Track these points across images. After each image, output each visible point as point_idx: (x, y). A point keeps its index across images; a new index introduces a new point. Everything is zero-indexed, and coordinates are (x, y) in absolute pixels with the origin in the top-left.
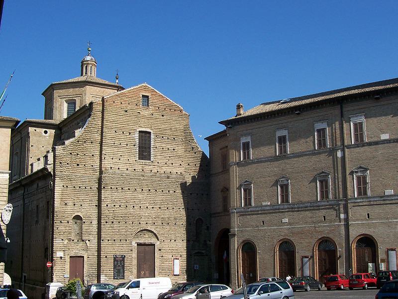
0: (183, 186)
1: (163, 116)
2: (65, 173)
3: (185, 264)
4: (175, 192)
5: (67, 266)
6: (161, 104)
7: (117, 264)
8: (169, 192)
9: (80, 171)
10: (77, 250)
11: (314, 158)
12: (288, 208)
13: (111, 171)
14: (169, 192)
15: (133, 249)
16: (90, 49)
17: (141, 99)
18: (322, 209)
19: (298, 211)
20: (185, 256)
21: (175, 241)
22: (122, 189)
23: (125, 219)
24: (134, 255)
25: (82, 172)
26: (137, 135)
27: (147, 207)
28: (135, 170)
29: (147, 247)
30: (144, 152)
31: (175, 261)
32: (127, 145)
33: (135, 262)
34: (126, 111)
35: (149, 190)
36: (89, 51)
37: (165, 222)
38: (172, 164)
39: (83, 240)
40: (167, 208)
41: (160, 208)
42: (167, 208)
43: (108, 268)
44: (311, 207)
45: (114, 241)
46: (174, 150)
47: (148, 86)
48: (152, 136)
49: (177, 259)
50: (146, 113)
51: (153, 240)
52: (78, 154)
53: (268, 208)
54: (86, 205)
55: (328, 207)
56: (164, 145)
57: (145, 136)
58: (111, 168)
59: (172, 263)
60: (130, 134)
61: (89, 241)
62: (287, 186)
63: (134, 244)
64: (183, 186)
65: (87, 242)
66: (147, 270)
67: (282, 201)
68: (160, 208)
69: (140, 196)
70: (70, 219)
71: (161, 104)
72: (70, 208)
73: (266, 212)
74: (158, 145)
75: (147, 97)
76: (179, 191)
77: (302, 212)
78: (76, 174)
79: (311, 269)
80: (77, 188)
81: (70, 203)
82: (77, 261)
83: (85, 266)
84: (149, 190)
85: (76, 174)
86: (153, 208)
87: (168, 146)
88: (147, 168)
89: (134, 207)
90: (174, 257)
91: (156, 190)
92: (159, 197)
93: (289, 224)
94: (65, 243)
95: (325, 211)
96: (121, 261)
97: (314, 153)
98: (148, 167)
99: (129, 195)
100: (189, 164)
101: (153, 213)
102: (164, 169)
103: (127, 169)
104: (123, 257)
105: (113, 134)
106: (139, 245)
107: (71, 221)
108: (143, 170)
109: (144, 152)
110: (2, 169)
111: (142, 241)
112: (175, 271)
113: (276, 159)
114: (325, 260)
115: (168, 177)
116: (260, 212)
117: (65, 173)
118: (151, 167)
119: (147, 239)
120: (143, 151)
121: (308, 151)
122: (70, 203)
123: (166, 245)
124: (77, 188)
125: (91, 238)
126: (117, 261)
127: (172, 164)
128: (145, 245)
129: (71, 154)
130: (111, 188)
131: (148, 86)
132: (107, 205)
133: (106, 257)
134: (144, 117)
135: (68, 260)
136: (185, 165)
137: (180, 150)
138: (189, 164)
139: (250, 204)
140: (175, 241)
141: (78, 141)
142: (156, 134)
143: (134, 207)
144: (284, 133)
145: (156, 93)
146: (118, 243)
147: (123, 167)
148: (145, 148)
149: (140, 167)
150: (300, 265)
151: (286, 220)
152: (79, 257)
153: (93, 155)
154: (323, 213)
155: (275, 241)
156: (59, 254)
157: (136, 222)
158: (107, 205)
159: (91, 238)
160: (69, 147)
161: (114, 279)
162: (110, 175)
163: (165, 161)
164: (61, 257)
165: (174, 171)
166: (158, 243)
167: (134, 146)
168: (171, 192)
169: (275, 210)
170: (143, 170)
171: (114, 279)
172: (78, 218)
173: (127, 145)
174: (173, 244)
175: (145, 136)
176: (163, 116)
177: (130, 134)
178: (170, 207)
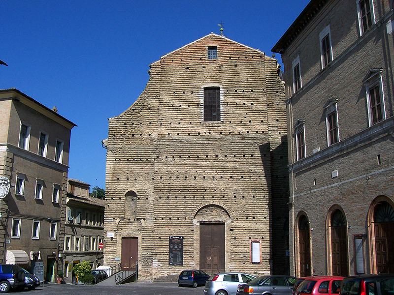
0: (265, 149)
1: (236, 66)
2: (119, 146)
3: (268, 248)
4: (252, 156)
5: (119, 248)
6: (232, 53)
7: (174, 246)
8: (244, 156)
9: (137, 141)
10: (129, 230)
11: (361, 53)
12: (337, 152)
13: (167, 138)
14: (244, 156)
15: (195, 229)
16: (222, 29)
17: (206, 52)
18: (375, 142)
19: (348, 154)
20: (267, 238)
21: (254, 218)
22: (180, 157)
23: (183, 193)
24: (196, 236)
25: (139, 142)
26: (201, 94)
27: (214, 177)
28: (199, 133)
29: (215, 228)
30: (212, 111)
31: (254, 244)
32: (189, 106)
33: (197, 245)
34: (188, 68)
35: (217, 156)
36: (222, 31)
37: (239, 195)
38: (250, 121)
39: (138, 219)
40: (242, 177)
41: (231, 177)
42: (242, 177)
43: (162, 251)
44: (361, 142)
45: (170, 219)
46: (252, 104)
47: (216, 35)
48: (222, 92)
49: (256, 242)
50: (213, 66)
51: (222, 218)
52: (133, 124)
53: (318, 157)
54: (141, 179)
55: (382, 136)
56: (244, 101)
57: (212, 94)
58: (169, 134)
59: (250, 247)
60: (192, 93)
61: (144, 219)
62: (334, 114)
63: (196, 223)
64: (265, 149)
65: (142, 220)
66: (215, 256)
67: (332, 142)
68: (231, 177)
69: (204, 164)
70: (123, 196)
71: (232, 53)
72: (122, 183)
73: (317, 163)
74: (229, 101)
75: (215, 48)
76: (258, 155)
77: (352, 155)
78: (129, 146)
79: (365, 258)
80: (131, 160)
81: (123, 178)
82: (130, 243)
83: (140, 249)
84: (217, 156)
85: (129, 146)
86: (221, 177)
87: (244, 101)
88: (216, 130)
89: (195, 177)
90: (253, 240)
91: (226, 156)
92: (231, 164)
93: (339, 178)
94: (117, 221)
95: (379, 144)
96: (178, 243)
97: (360, 44)
98: (216, 128)
99: (188, 163)
100: (277, 120)
101: (222, 184)
102: (239, 129)
103: (189, 134)
104: (181, 239)
105: (172, 96)
106: (202, 224)
107: (124, 198)
108: (210, 133)
109: (212, 111)
110: (2, 142)
111: (207, 219)
112: (253, 257)
113: (323, 74)
114: (384, 242)
115: (243, 138)
116: (312, 166)
117: (119, 146)
118: (220, 129)
119: (212, 217)
120: (211, 111)
121: (352, 46)
122: (123, 178)
123: (241, 224)
124: (131, 160)
125: (147, 216)
126: (174, 243)
127: (250, 121)
128: (210, 224)
129: (125, 124)
130: (166, 157)
131: (216, 35)
132: (161, 177)
133: (160, 238)
134: (210, 70)
135: (119, 241)
136: (272, 123)
137: (261, 103)
138: (277, 120)
139: (304, 156)
140: (254, 218)
141: (134, 110)
142: (227, 88)
143: (195, 177)
144: (327, 31)
145: (227, 41)
146: (174, 222)
147: (183, 132)
148: (214, 107)
149: (206, 130)
150: (353, 252)
151: (336, 173)
152: (132, 238)
153: (150, 123)
154: (374, 150)
155: (326, 210)
156: (110, 234)
157: (199, 196)
158: (161, 177)
159: (147, 216)
160: (124, 117)
161: (169, 264)
162: (166, 143)
163: (240, 119)
164: (112, 238)
165: (254, 130)
166: (229, 221)
167: (198, 105)
168: (247, 156)
169: (325, 158)
170: (210, 133)
171: (169, 264)
172: (131, 194)
173: (189, 106)
174: (250, 223)
175: (212, 94)
176: (236, 66)
177: (192, 93)
178: (246, 174)
